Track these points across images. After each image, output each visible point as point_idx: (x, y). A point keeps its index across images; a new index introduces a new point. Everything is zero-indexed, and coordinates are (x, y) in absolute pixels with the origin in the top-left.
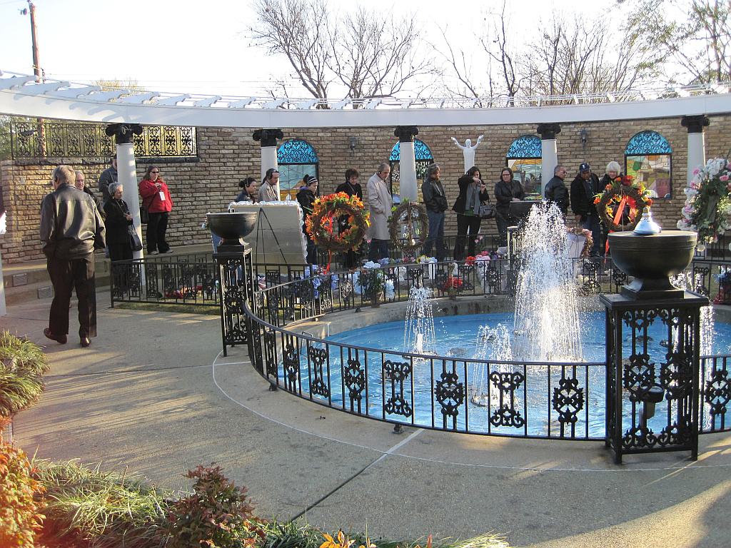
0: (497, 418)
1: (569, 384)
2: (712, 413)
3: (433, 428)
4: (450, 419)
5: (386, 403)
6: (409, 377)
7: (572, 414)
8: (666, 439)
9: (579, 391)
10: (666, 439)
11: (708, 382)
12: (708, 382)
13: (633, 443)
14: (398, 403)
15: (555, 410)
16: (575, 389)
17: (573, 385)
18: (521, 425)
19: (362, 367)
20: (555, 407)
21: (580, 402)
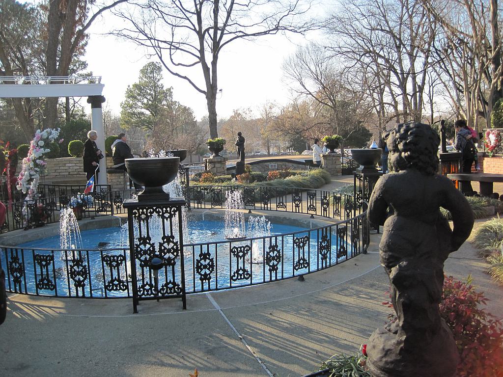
0: (110, 286)
1: (205, 256)
2: (270, 270)
3: (70, 297)
4: (80, 289)
5: (38, 282)
6: (51, 264)
7: (208, 275)
8: (142, 292)
9: (212, 260)
10: (142, 292)
11: (267, 252)
12: (267, 252)
13: (143, 294)
14: (45, 282)
15: (198, 274)
16: (209, 259)
17: (208, 256)
18: (125, 289)
19: (21, 261)
20: (198, 272)
21: (212, 266)
